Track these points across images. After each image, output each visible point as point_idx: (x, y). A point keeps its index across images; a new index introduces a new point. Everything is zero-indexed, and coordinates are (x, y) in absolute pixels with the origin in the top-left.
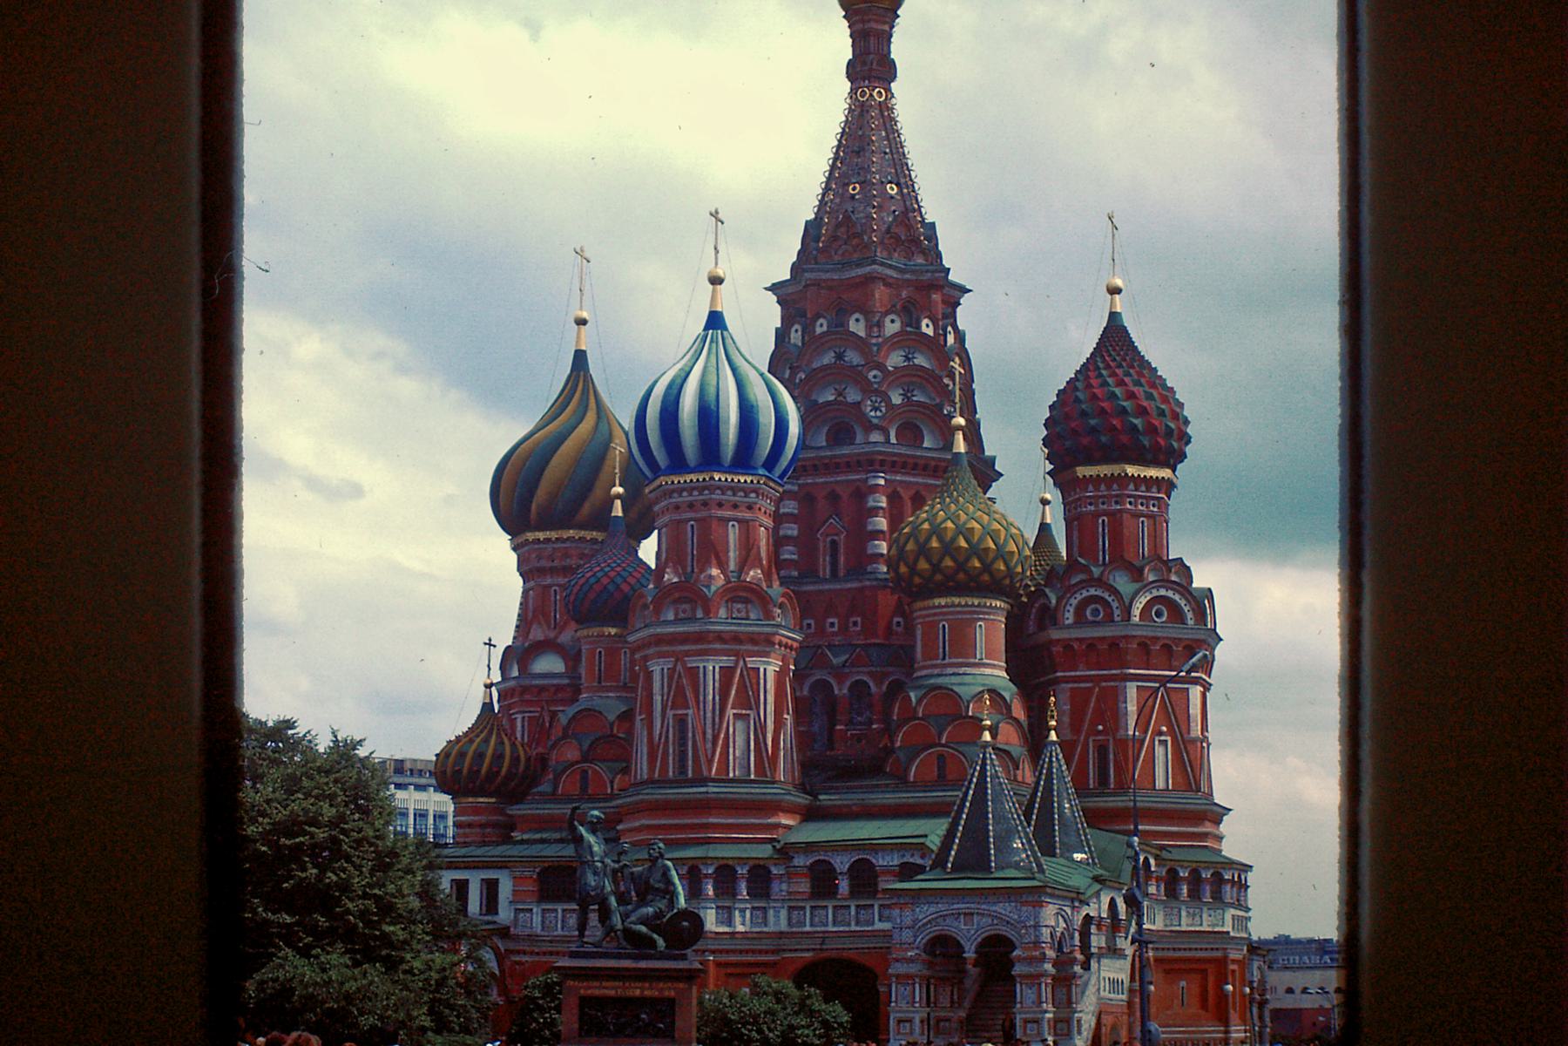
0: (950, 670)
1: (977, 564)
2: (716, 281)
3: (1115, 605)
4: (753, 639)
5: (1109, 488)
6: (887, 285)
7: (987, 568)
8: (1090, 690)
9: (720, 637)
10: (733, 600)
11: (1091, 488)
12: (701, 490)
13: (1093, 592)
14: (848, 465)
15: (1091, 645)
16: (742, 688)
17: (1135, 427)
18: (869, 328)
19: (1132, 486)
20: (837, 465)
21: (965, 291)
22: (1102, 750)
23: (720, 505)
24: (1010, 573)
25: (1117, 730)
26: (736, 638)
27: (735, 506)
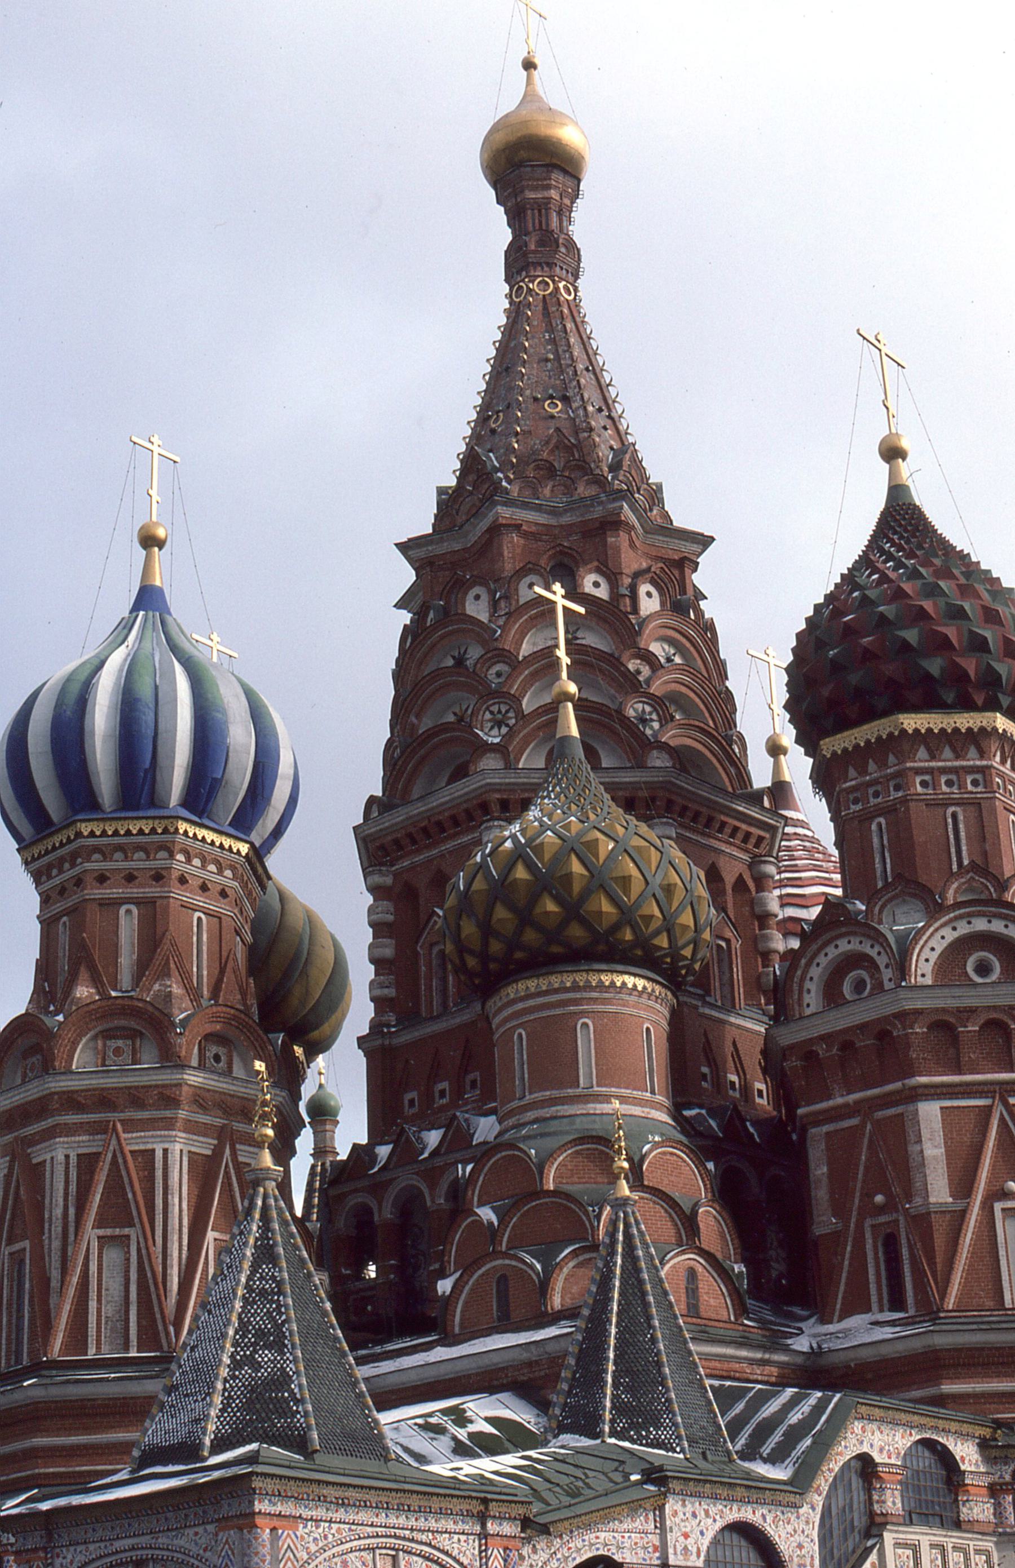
0: (531, 1115)
1: (551, 906)
2: (149, 541)
3: (882, 961)
4: (136, 1097)
5: (883, 764)
6: (526, 535)
7: (574, 910)
8: (855, 1132)
9: (71, 1101)
10: (107, 1035)
11: (852, 772)
12: (73, 858)
13: (844, 946)
14: (455, 821)
15: (845, 1043)
16: (116, 1187)
17: (906, 646)
18: (494, 605)
19: (922, 753)
20: (441, 827)
21: (705, 541)
22: (891, 1243)
23: (102, 879)
24: (627, 915)
25: (909, 1197)
26: (104, 1100)
27: (130, 878)
